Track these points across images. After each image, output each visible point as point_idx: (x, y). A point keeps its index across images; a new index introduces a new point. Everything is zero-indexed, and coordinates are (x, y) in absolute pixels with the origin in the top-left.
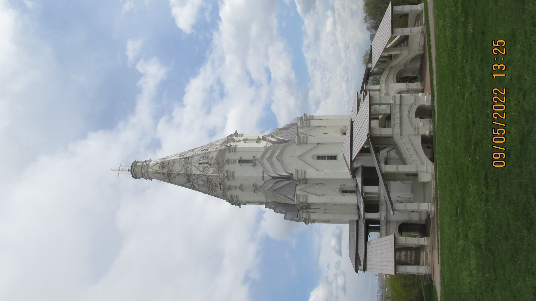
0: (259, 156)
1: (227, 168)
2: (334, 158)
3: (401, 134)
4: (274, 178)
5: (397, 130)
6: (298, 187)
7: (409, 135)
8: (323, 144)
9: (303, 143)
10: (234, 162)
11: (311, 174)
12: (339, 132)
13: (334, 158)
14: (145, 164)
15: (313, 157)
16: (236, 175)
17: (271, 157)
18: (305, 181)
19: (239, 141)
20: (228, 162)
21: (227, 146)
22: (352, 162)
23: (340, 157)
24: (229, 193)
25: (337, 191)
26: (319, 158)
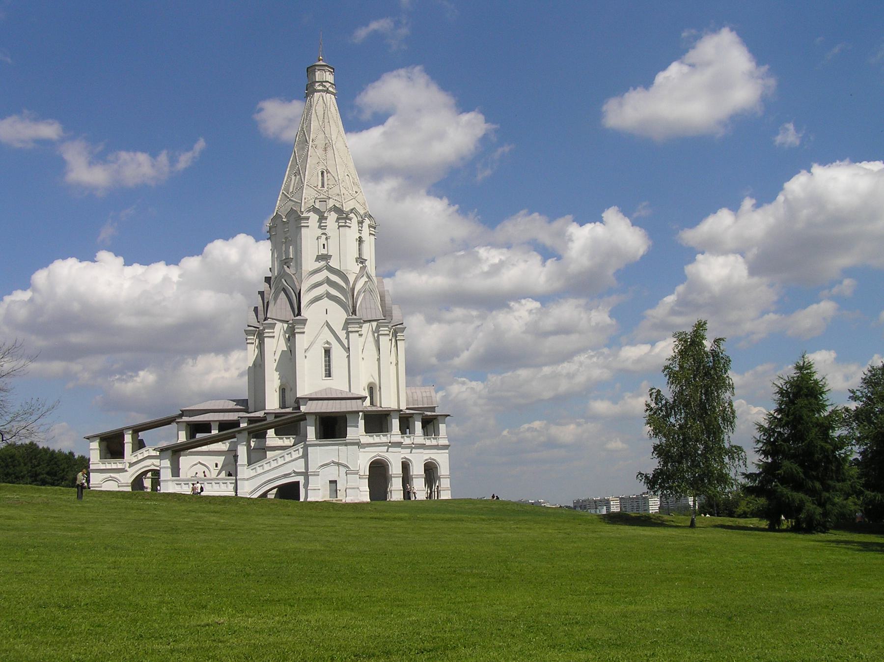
0: (333, 263)
1: (314, 218)
2: (328, 374)
11: (301, 341)
12: (372, 380)
13: (328, 374)
14: (327, 85)
16: (303, 230)
17: (328, 281)
20: (322, 218)
21: (347, 215)
23: (329, 383)
26: (327, 352)
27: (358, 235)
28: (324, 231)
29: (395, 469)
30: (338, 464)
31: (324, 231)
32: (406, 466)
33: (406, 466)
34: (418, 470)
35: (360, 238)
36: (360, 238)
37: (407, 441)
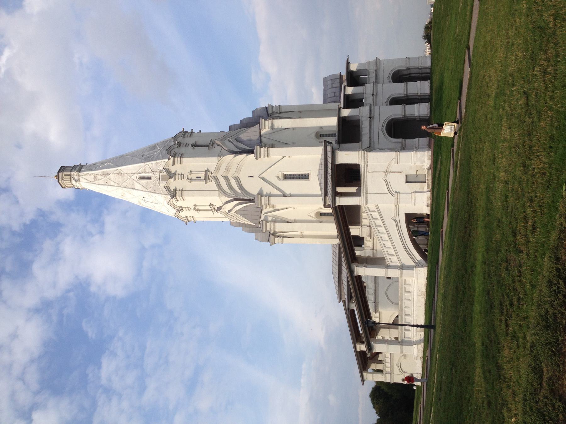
2: (306, 177)
13: (306, 177)
15: (278, 177)
19: (187, 145)
25: (313, 215)
26: (287, 177)
27: (190, 148)
28: (185, 177)
29: (397, 111)
30: (387, 172)
31: (185, 177)
32: (395, 101)
33: (395, 101)
34: (399, 89)
35: (193, 145)
36: (193, 145)
37: (368, 100)
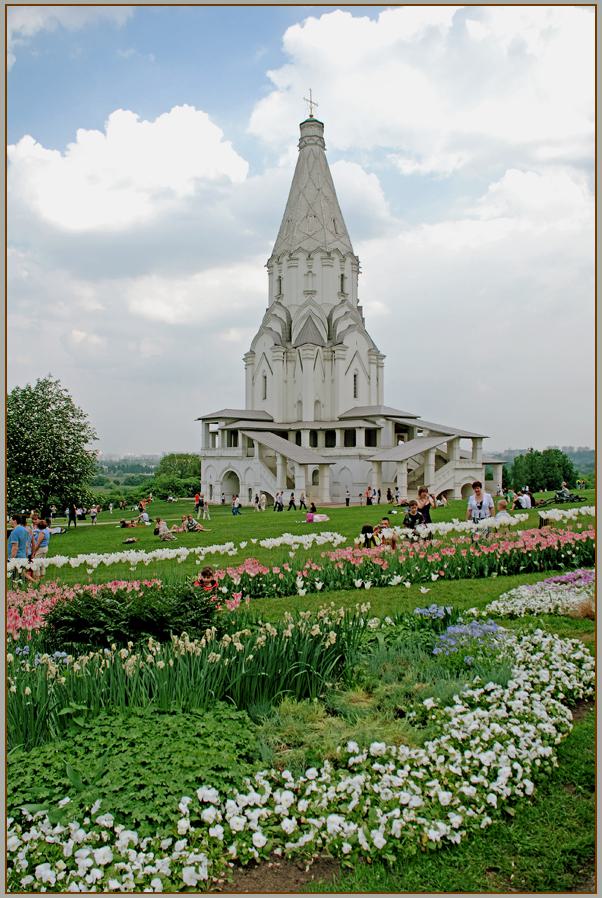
3: (456, 469)
4: (329, 320)
5: (458, 466)
6: (320, 348)
7: (454, 477)
8: (369, 383)
9: (370, 359)
10: (342, 269)
11: (341, 365)
18: (333, 359)
22: (385, 417)
24: (302, 257)
25: (317, 398)
